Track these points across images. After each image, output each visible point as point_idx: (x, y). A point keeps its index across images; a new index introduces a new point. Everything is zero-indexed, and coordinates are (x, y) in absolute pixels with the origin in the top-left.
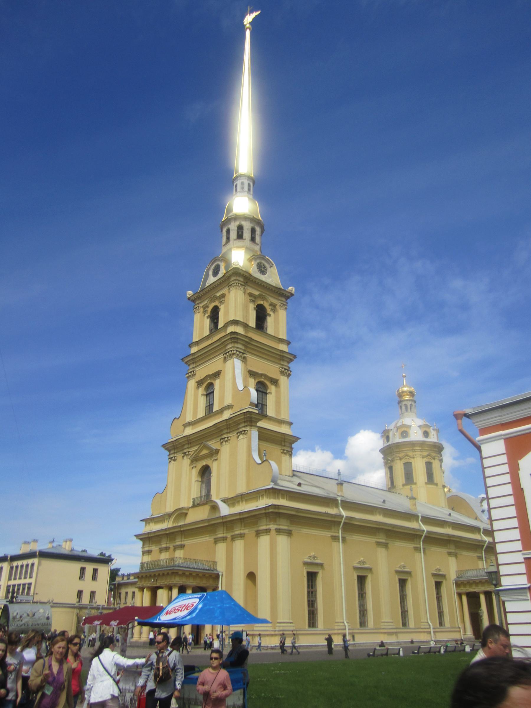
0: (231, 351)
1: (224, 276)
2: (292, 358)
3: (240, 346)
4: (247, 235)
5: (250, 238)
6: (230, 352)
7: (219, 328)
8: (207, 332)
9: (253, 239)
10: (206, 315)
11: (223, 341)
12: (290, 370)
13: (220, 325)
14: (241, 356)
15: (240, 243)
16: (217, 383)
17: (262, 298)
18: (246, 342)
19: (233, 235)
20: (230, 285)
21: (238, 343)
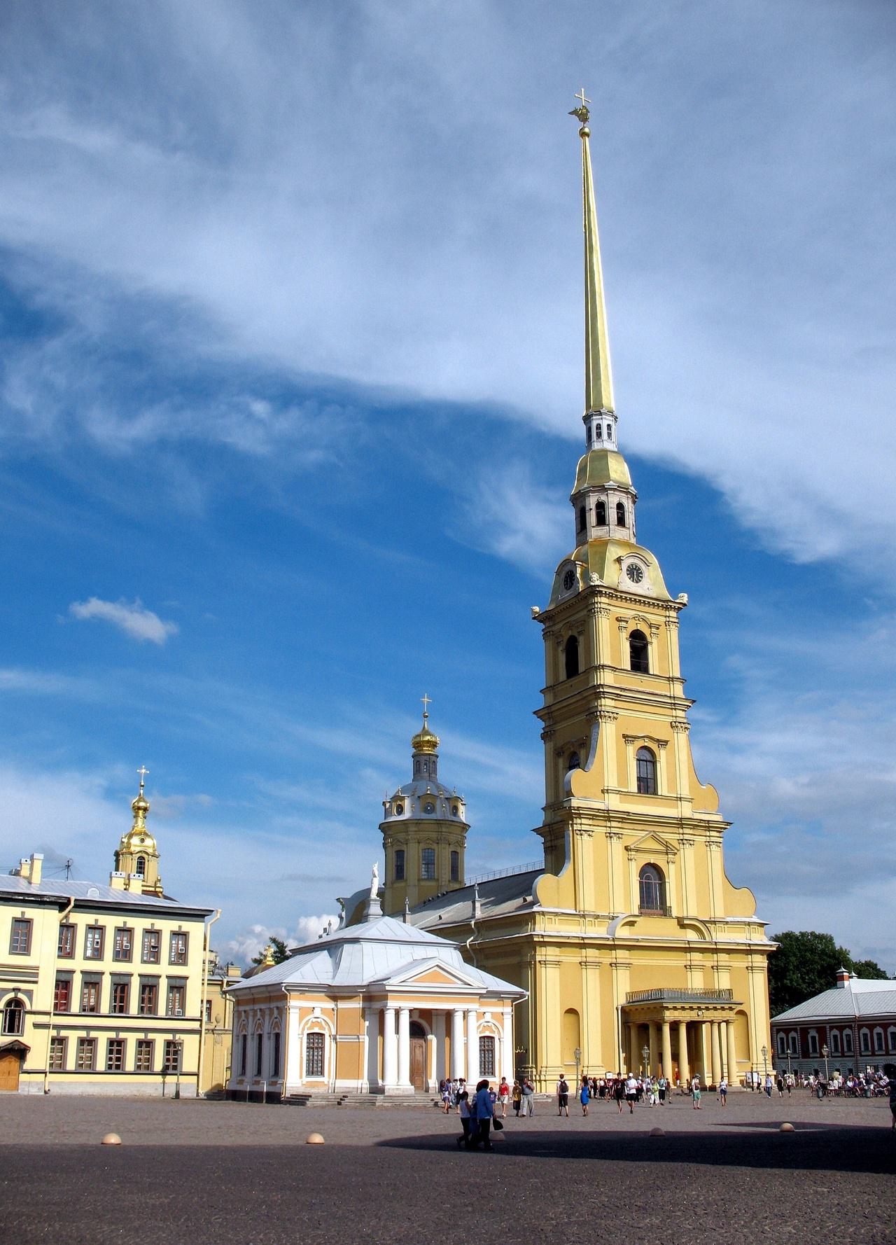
0: (596, 712)
4: (612, 515)
8: (563, 675)
9: (621, 522)
10: (561, 648)
11: (587, 694)
13: (581, 668)
16: (582, 753)
19: (592, 518)
21: (604, 698)
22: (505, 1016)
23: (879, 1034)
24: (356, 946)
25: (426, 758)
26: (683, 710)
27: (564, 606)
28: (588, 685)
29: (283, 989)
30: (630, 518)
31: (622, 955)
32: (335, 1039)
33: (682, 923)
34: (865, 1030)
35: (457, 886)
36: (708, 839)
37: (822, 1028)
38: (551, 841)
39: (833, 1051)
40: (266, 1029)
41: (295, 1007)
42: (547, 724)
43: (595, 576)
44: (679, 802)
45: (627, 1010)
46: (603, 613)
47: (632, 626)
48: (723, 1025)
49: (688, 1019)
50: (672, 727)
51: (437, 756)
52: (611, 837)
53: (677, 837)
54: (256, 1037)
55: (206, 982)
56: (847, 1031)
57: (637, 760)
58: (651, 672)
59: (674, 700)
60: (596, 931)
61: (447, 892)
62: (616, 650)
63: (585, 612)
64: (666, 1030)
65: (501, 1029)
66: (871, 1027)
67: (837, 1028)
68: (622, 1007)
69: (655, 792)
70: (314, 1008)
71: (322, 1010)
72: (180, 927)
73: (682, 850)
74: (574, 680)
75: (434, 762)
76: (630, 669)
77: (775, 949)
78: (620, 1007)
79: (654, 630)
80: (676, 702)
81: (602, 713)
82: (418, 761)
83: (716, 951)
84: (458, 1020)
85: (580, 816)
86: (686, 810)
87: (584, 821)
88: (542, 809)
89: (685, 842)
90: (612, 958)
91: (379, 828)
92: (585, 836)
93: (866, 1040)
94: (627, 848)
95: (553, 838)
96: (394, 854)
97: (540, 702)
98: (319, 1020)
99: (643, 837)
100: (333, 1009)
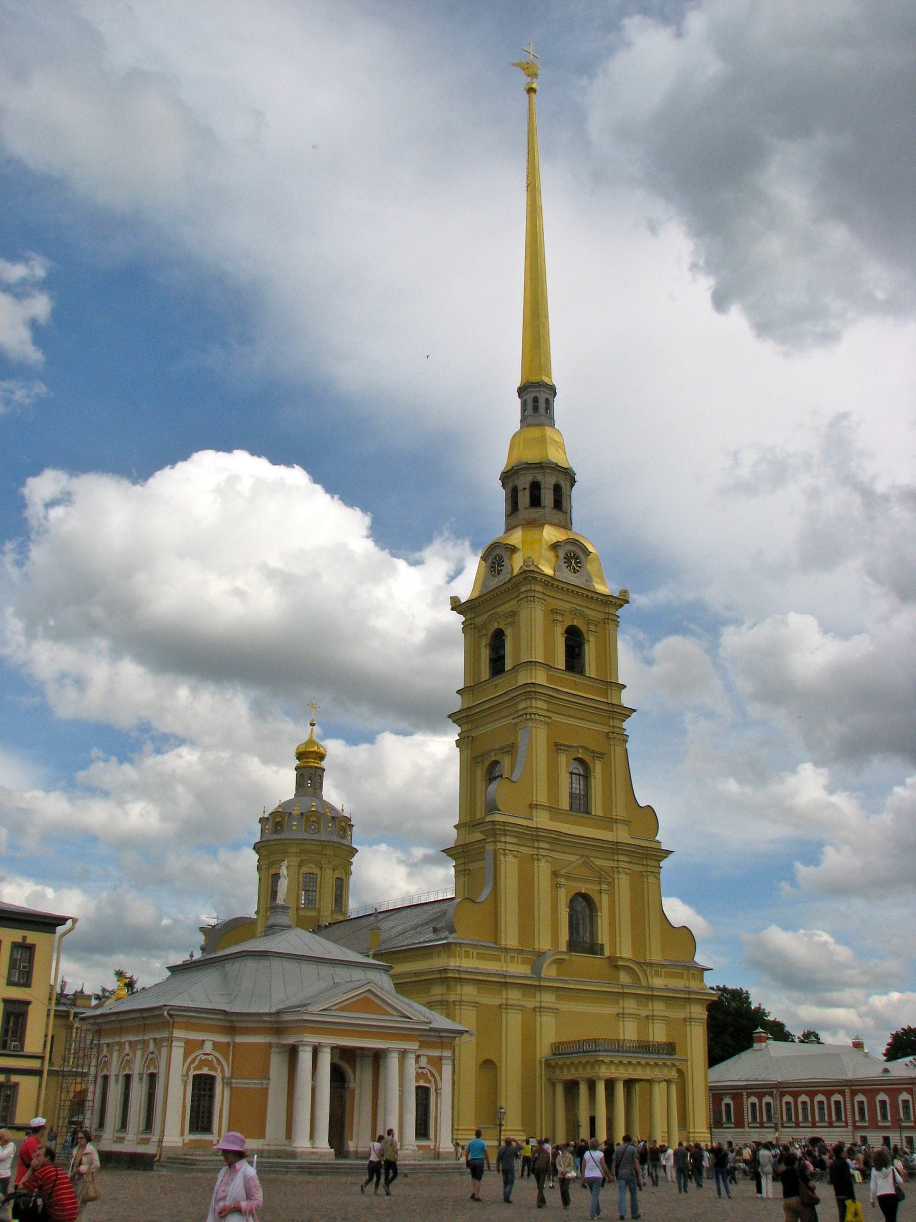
0: (526, 714)
1: (508, 581)
2: (627, 713)
3: (541, 704)
4: (547, 497)
6: (525, 716)
7: (506, 670)
10: (484, 643)
11: (512, 695)
12: (625, 733)
13: (508, 666)
15: (534, 513)
16: (506, 761)
17: (575, 614)
18: (551, 696)
19: (524, 499)
20: (521, 599)
21: (536, 699)
22: (444, 1062)
23: (804, 1103)
24: (264, 963)
25: (312, 771)
27: (490, 595)
28: (517, 682)
29: (165, 1014)
31: (548, 999)
32: (231, 1083)
33: (614, 964)
34: (788, 1098)
35: (341, 918)
36: (645, 867)
37: (737, 1093)
38: (465, 863)
39: (750, 1120)
40: (137, 1068)
41: (179, 1039)
42: (466, 728)
44: (615, 824)
45: (553, 1063)
48: (664, 1084)
49: (626, 1076)
50: (608, 738)
51: (324, 770)
52: (539, 860)
53: (611, 864)
54: (121, 1080)
55: (52, 1013)
56: (767, 1099)
57: (571, 773)
59: (612, 708)
60: (518, 969)
61: (330, 924)
63: (514, 602)
64: (601, 1088)
65: (438, 1077)
66: (795, 1095)
67: (755, 1094)
68: (546, 1060)
69: (588, 812)
70: (203, 1041)
71: (214, 1043)
72: (25, 938)
73: (616, 881)
74: (500, 680)
75: (320, 776)
76: (564, 669)
77: (716, 999)
78: (544, 1060)
79: (592, 627)
80: (615, 710)
82: (302, 774)
84: (393, 1062)
85: (505, 833)
86: (622, 835)
87: (509, 839)
88: (455, 826)
90: (536, 1001)
91: (254, 849)
92: (510, 859)
93: (789, 1110)
94: (555, 874)
95: (467, 861)
96: (270, 878)
97: (457, 703)
98: (210, 1058)
99: (574, 862)
100: (228, 1044)
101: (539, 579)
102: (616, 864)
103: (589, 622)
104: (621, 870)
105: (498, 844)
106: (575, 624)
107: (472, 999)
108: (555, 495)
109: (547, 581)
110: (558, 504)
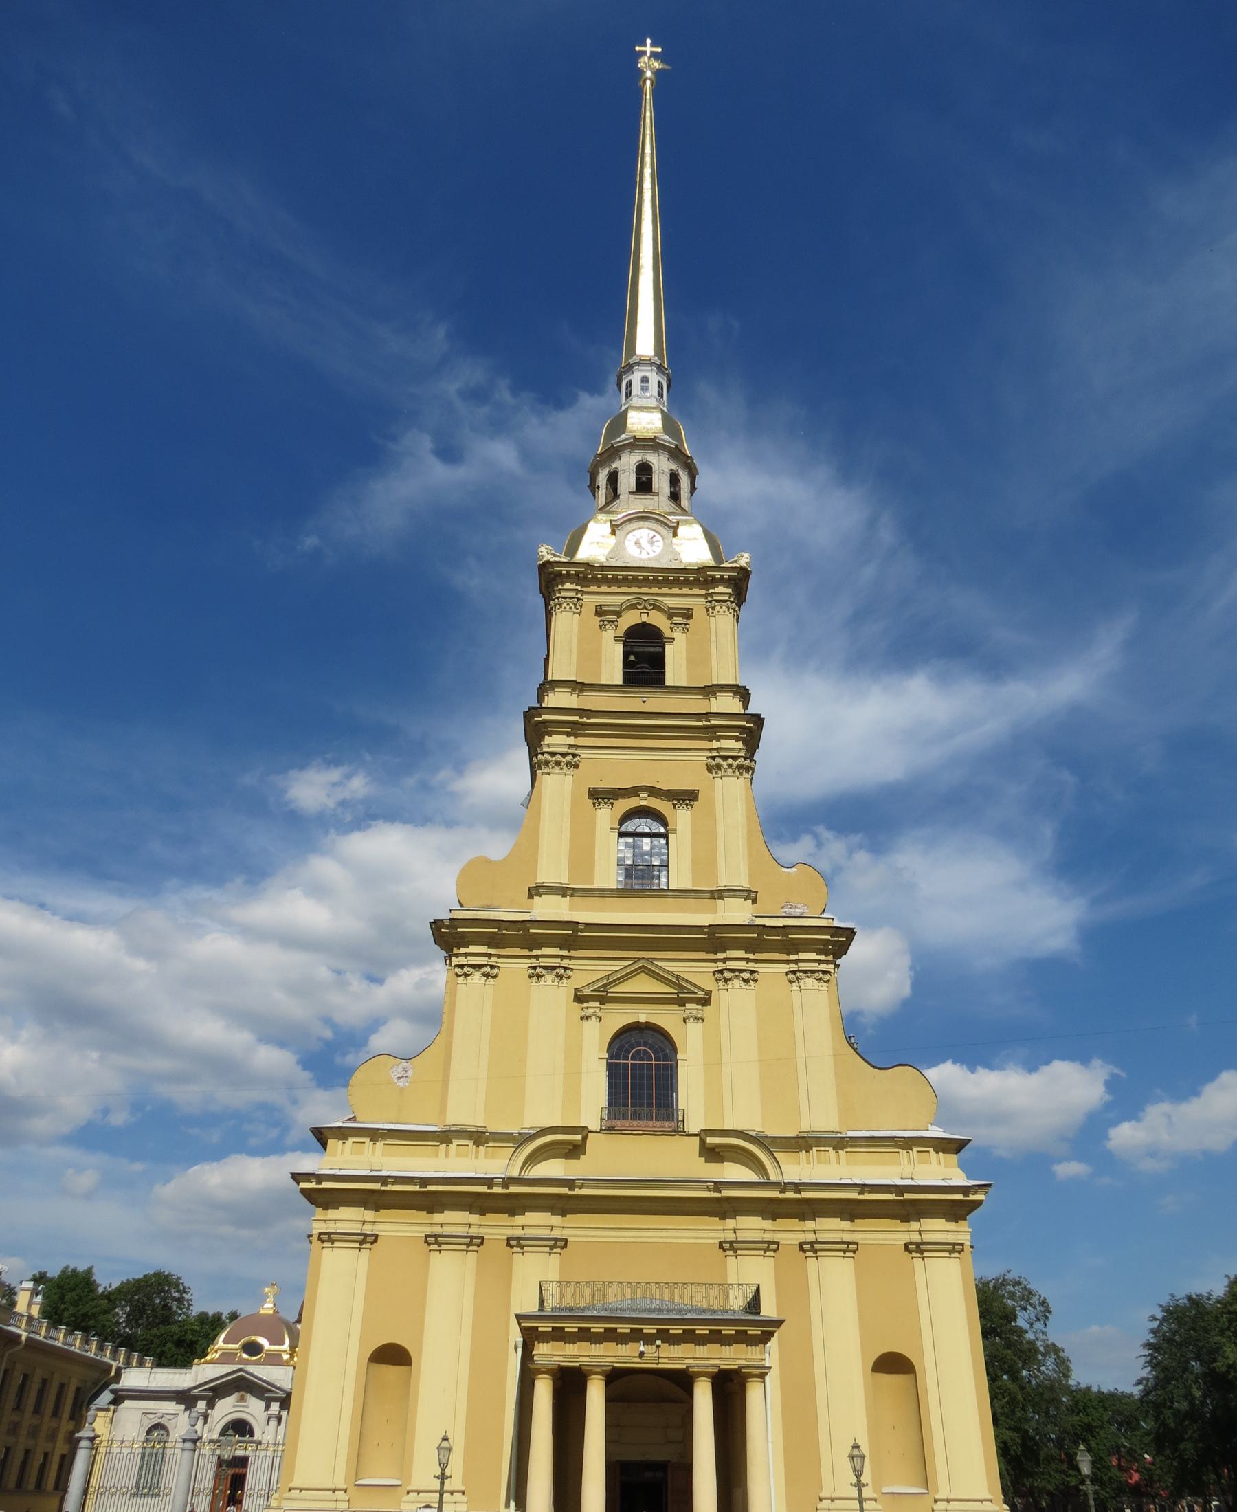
5: (635, 490)
14: (558, 763)
17: (645, 608)
21: (550, 734)
26: (737, 739)
30: (661, 483)
31: (537, 1222)
36: (793, 967)
43: (543, 549)
46: (565, 605)
47: (631, 619)
50: (709, 770)
52: (539, 976)
58: (667, 683)
62: (590, 655)
76: (621, 683)
79: (677, 619)
80: (713, 722)
81: (540, 757)
83: (807, 1210)
85: (464, 941)
86: (736, 913)
89: (728, 975)
92: (477, 977)
94: (579, 998)
99: (616, 971)
101: (564, 572)
102: (721, 966)
103: (671, 613)
104: (728, 975)
105: (453, 959)
106: (644, 618)
107: (356, 1228)
108: (638, 479)
109: (581, 572)
110: (644, 486)
